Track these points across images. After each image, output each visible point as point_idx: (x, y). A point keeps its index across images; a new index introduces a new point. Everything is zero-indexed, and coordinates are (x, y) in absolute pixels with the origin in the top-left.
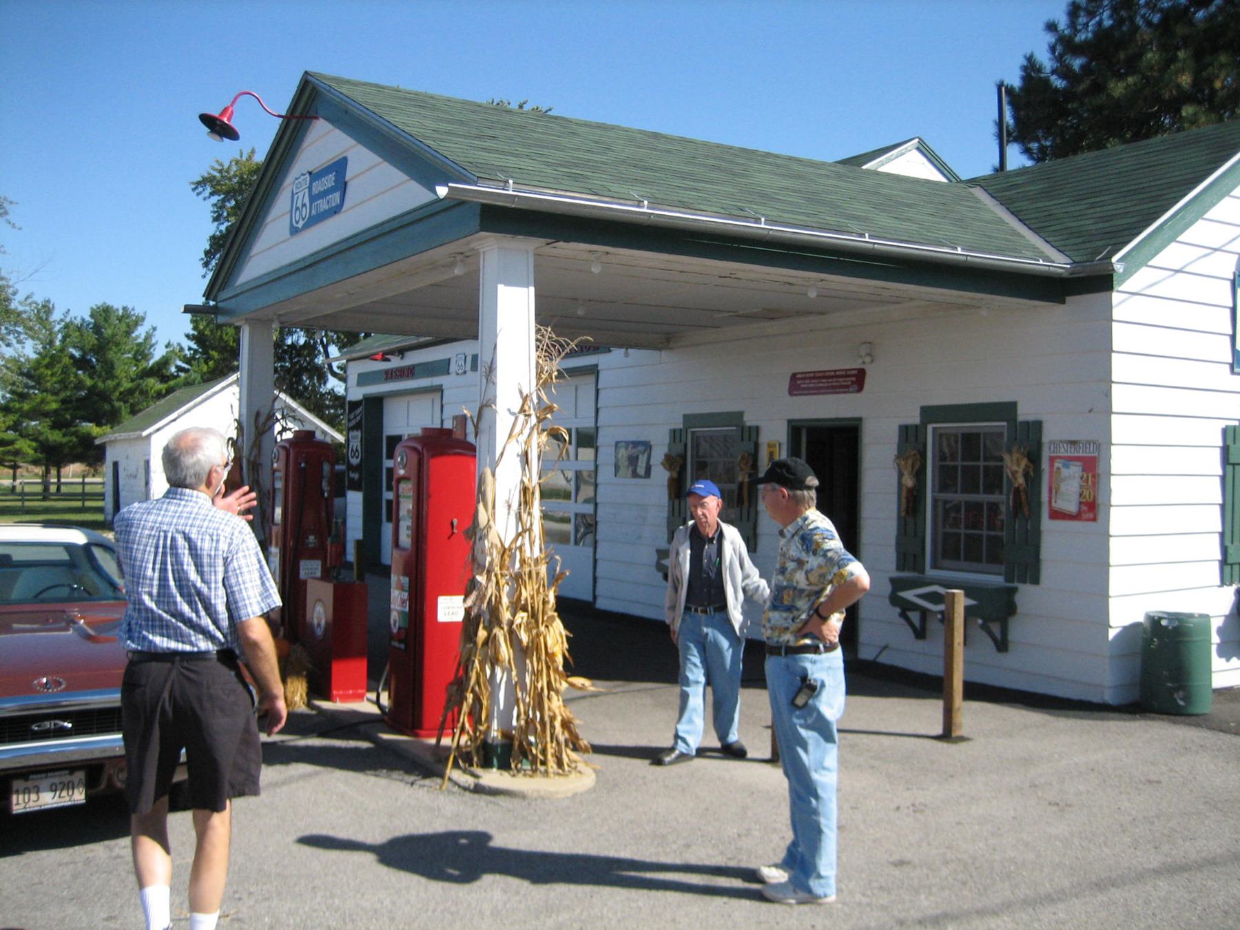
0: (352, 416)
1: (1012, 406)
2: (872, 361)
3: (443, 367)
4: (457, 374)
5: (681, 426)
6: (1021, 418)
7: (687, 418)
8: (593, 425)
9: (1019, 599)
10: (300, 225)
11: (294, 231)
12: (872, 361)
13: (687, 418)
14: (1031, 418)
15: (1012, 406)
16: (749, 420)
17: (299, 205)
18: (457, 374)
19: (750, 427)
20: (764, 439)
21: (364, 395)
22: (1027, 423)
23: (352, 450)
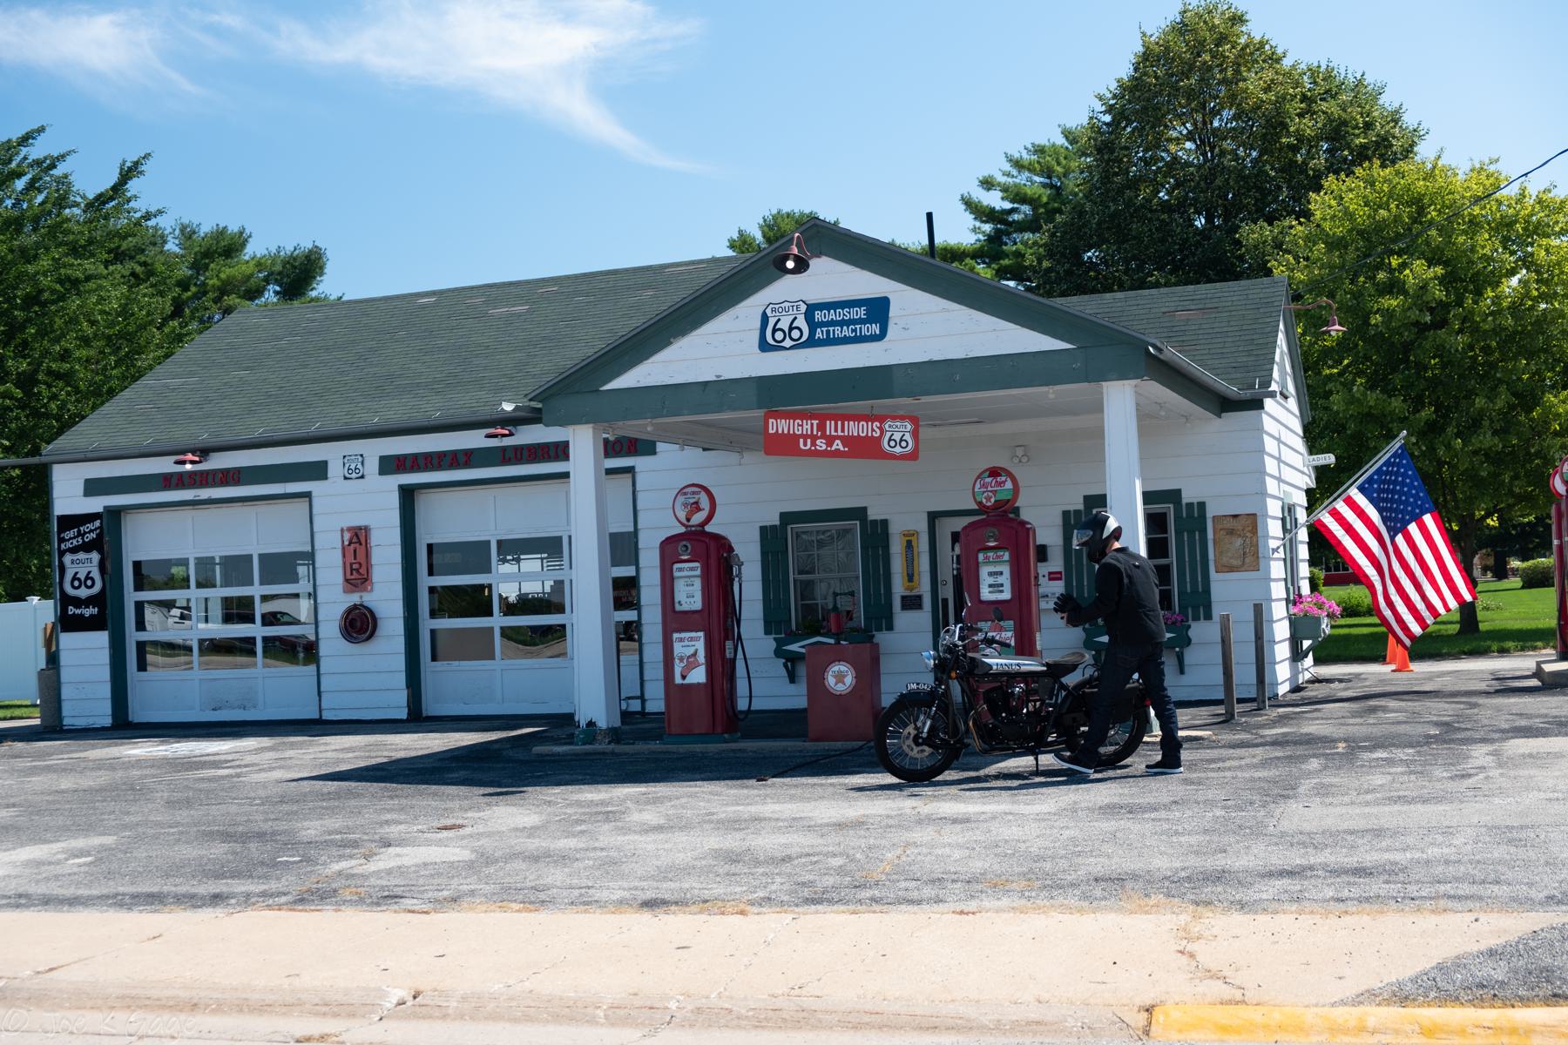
0: (71, 534)
1: (1178, 493)
2: (1028, 461)
3: (318, 471)
4: (346, 478)
5: (778, 523)
6: (1184, 501)
7: (782, 515)
8: (632, 529)
9: (1191, 633)
10: (788, 343)
11: (764, 346)
12: (1028, 461)
13: (783, 515)
14: (1195, 501)
15: (1178, 493)
16: (874, 514)
17: (784, 325)
18: (346, 478)
19: (874, 522)
20: (895, 529)
21: (105, 507)
22: (876, 521)
23: (75, 578)
